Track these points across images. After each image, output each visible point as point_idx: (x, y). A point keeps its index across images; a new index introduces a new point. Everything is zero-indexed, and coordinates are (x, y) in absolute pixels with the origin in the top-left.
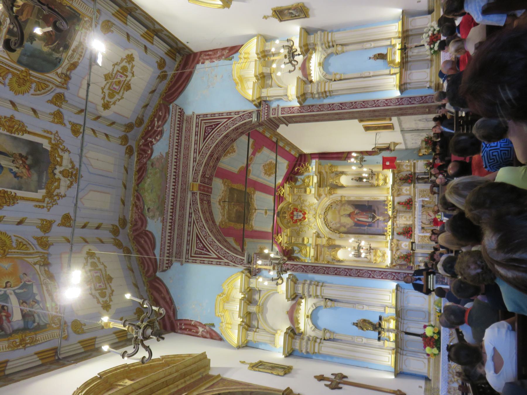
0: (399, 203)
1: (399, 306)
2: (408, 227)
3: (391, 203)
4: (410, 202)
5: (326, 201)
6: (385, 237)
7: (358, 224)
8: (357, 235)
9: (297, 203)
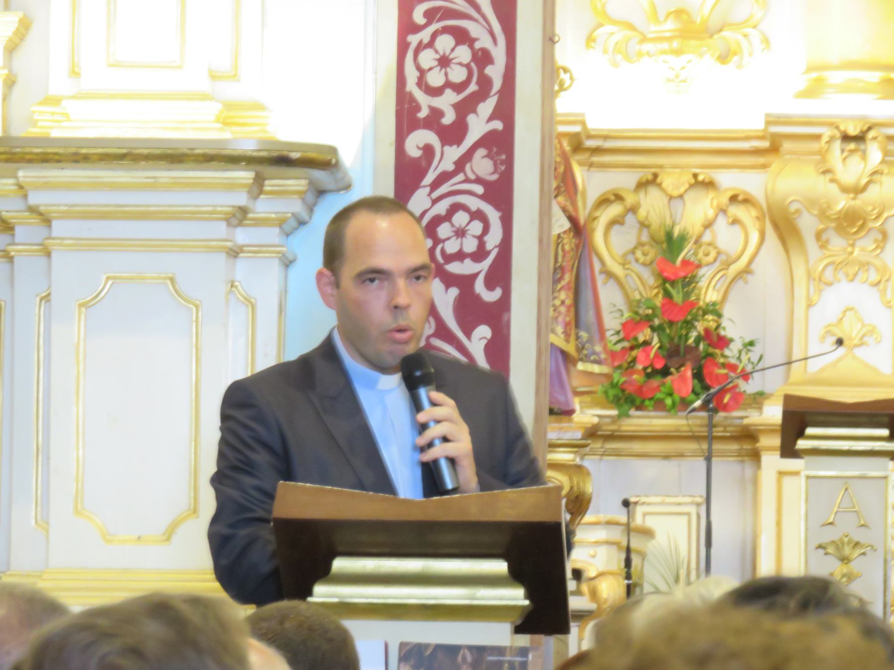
1: (51, 188)
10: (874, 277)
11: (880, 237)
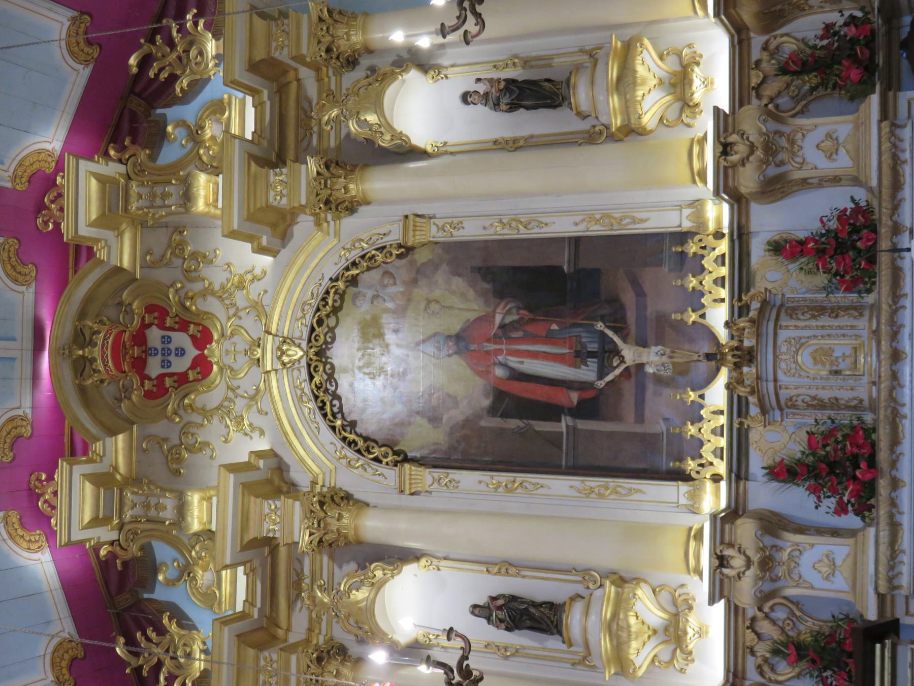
0: (785, 249)
2: (845, 418)
3: (723, 247)
4: (856, 230)
5: (319, 252)
6: (684, 487)
7: (516, 401)
8: (504, 478)
9: (162, 275)
10: (797, 553)
11: (774, 549)
